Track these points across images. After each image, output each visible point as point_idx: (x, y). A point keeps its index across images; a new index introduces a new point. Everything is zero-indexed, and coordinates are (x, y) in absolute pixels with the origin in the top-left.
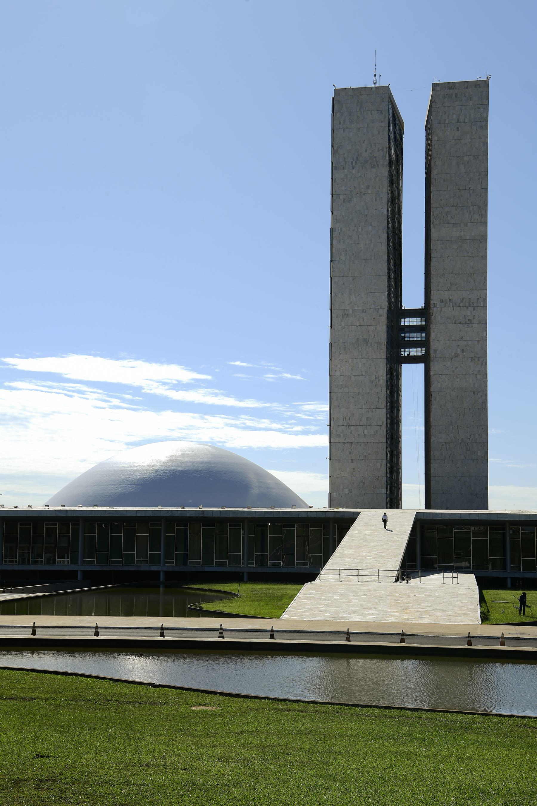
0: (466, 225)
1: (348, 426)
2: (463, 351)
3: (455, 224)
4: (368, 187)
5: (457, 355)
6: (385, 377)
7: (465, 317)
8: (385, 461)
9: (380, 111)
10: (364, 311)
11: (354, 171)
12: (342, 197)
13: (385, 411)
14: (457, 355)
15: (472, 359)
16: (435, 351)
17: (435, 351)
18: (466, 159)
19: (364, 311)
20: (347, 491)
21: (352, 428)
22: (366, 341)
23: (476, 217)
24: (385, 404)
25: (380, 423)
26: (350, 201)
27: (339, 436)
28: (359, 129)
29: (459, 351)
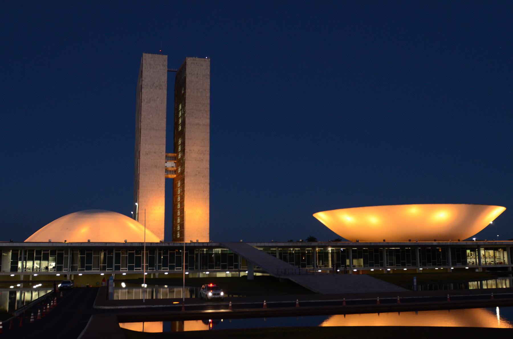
0: (200, 118)
2: (199, 173)
3: (196, 118)
4: (158, 98)
5: (196, 175)
7: (200, 158)
9: (163, 65)
10: (155, 153)
11: (151, 90)
12: (146, 101)
16: (187, 172)
18: (201, 90)
22: (156, 166)
28: (154, 72)
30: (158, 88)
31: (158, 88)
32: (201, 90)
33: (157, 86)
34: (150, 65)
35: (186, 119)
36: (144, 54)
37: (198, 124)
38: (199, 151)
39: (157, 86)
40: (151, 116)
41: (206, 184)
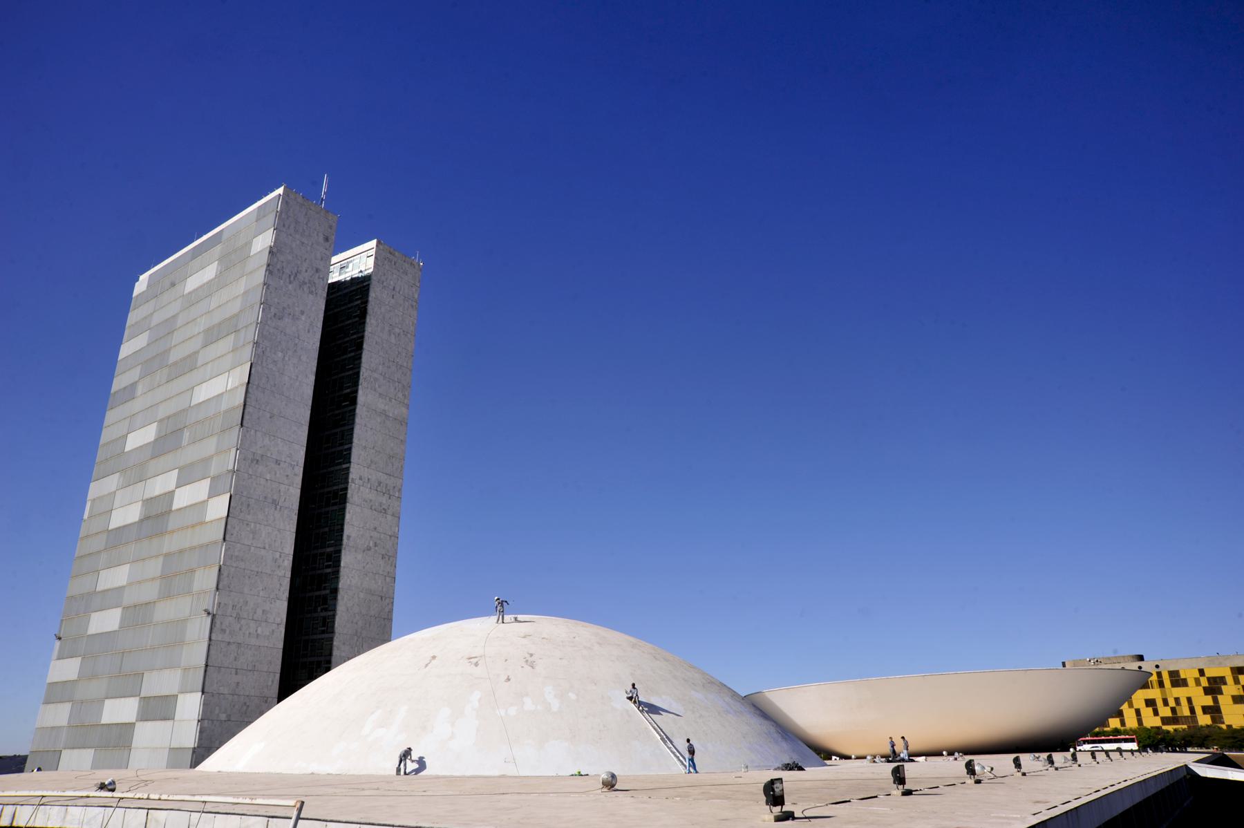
1: (238, 618)
2: (376, 545)
4: (302, 313)
5: (369, 549)
7: (381, 504)
8: (278, 676)
10: (277, 462)
13: (286, 604)
16: (349, 537)
18: (397, 330)
19: (277, 462)
20: (223, 717)
21: (243, 622)
23: (400, 395)
24: (287, 594)
25: (278, 620)
26: (280, 318)
27: (223, 631)
29: (371, 544)
33: (304, 283)
34: (297, 222)
35: (360, 392)
37: (384, 413)
38: (380, 483)
40: (280, 354)
41: (388, 579)
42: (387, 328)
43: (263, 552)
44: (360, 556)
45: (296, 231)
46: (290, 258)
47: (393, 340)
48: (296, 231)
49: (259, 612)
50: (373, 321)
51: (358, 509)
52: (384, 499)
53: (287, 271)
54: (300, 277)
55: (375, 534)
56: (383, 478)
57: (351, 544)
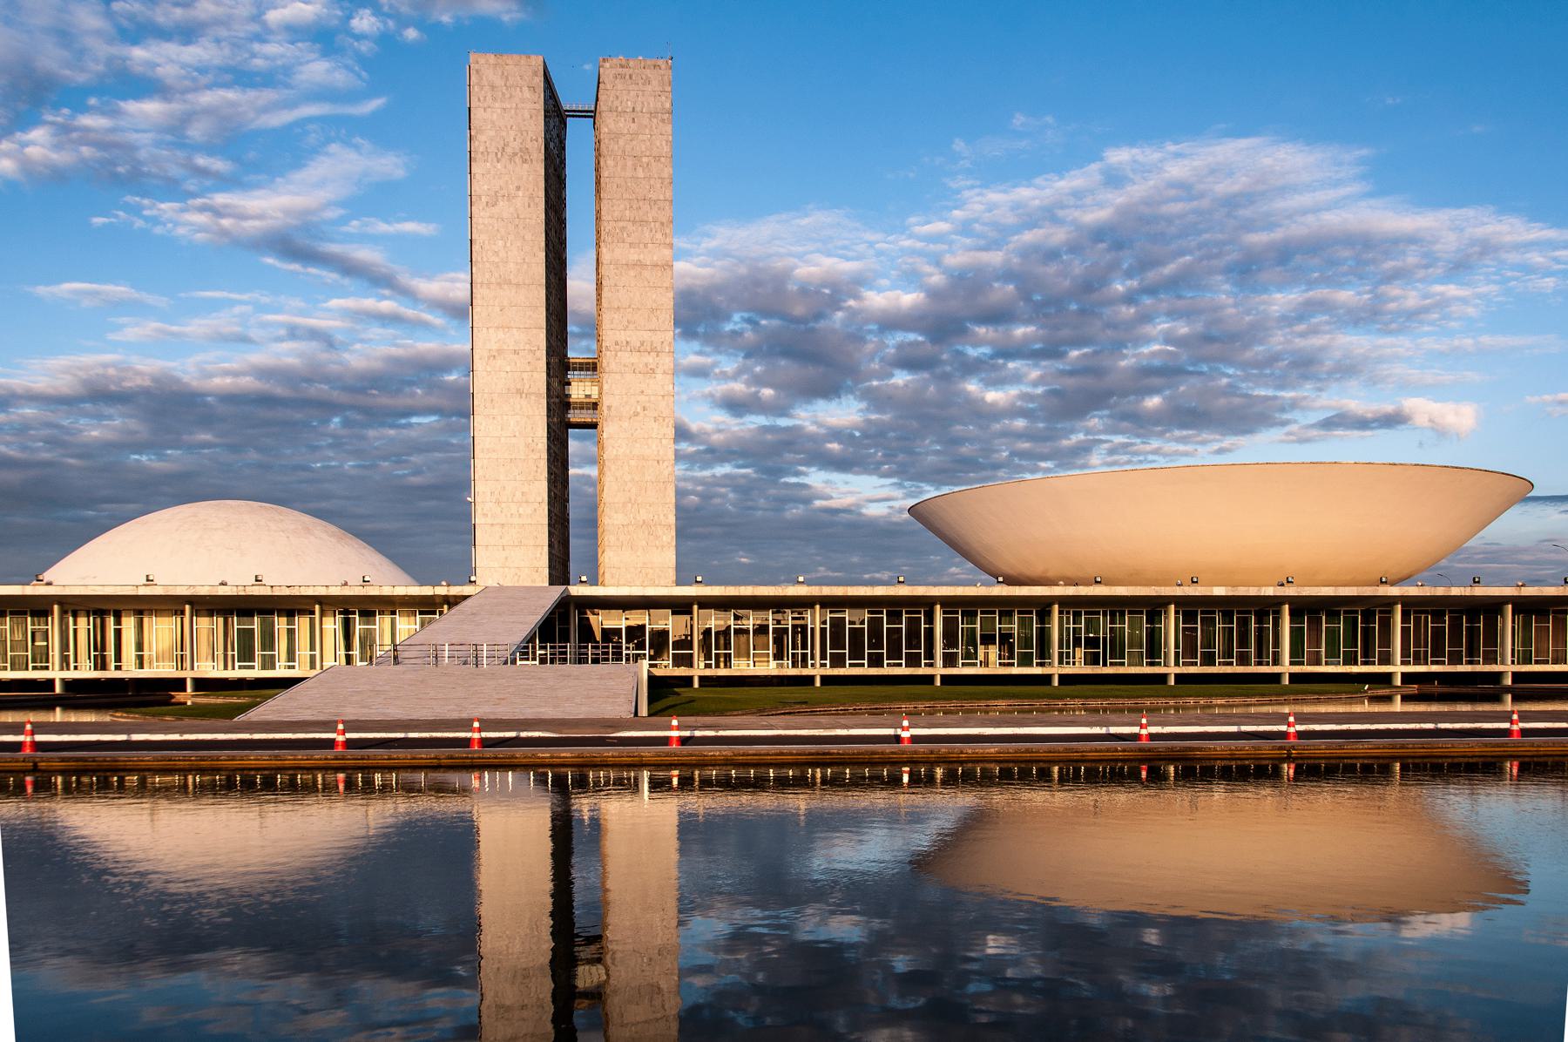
0: (646, 246)
1: (498, 502)
4: (518, 188)
5: (636, 414)
6: (545, 440)
9: (533, 89)
10: (516, 352)
12: (484, 199)
13: (545, 484)
14: (636, 414)
15: (656, 419)
16: (609, 408)
17: (609, 408)
18: (645, 160)
19: (516, 352)
22: (520, 392)
23: (659, 236)
27: (485, 515)
30: (517, 159)
31: (517, 159)
32: (645, 160)
33: (515, 154)
34: (493, 87)
36: (472, 57)
37: (639, 265)
39: (515, 154)
40: (500, 243)
42: (630, 163)
43: (514, 440)
44: (626, 425)
45: (494, 99)
46: (492, 133)
47: (640, 173)
48: (494, 99)
49: (518, 494)
50: (610, 162)
51: (618, 376)
52: (650, 359)
53: (492, 149)
54: (509, 150)
55: (642, 398)
56: (646, 336)
57: (613, 412)
